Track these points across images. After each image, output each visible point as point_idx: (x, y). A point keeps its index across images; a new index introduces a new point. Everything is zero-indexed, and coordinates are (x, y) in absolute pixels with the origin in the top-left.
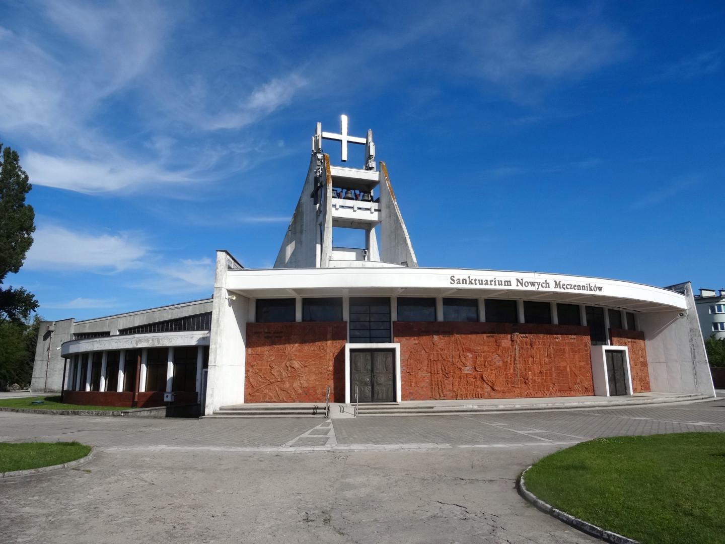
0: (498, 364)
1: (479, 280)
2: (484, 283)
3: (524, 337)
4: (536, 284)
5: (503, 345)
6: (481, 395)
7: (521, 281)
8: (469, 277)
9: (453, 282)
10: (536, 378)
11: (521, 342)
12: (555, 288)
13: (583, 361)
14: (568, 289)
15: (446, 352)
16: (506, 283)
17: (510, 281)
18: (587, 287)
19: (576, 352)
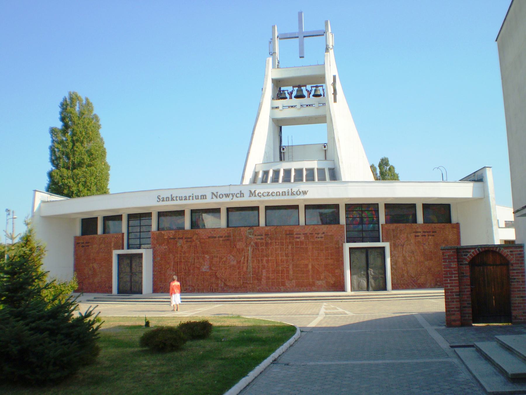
0: (232, 263)
1: (180, 197)
2: (183, 198)
3: (259, 239)
4: (231, 195)
5: (238, 247)
6: (215, 290)
7: (216, 194)
8: (172, 195)
9: (159, 200)
10: (271, 275)
11: (256, 244)
12: (250, 196)
13: (331, 259)
14: (264, 196)
15: (187, 255)
16: (202, 197)
17: (205, 195)
18: (288, 192)
19: (322, 251)
